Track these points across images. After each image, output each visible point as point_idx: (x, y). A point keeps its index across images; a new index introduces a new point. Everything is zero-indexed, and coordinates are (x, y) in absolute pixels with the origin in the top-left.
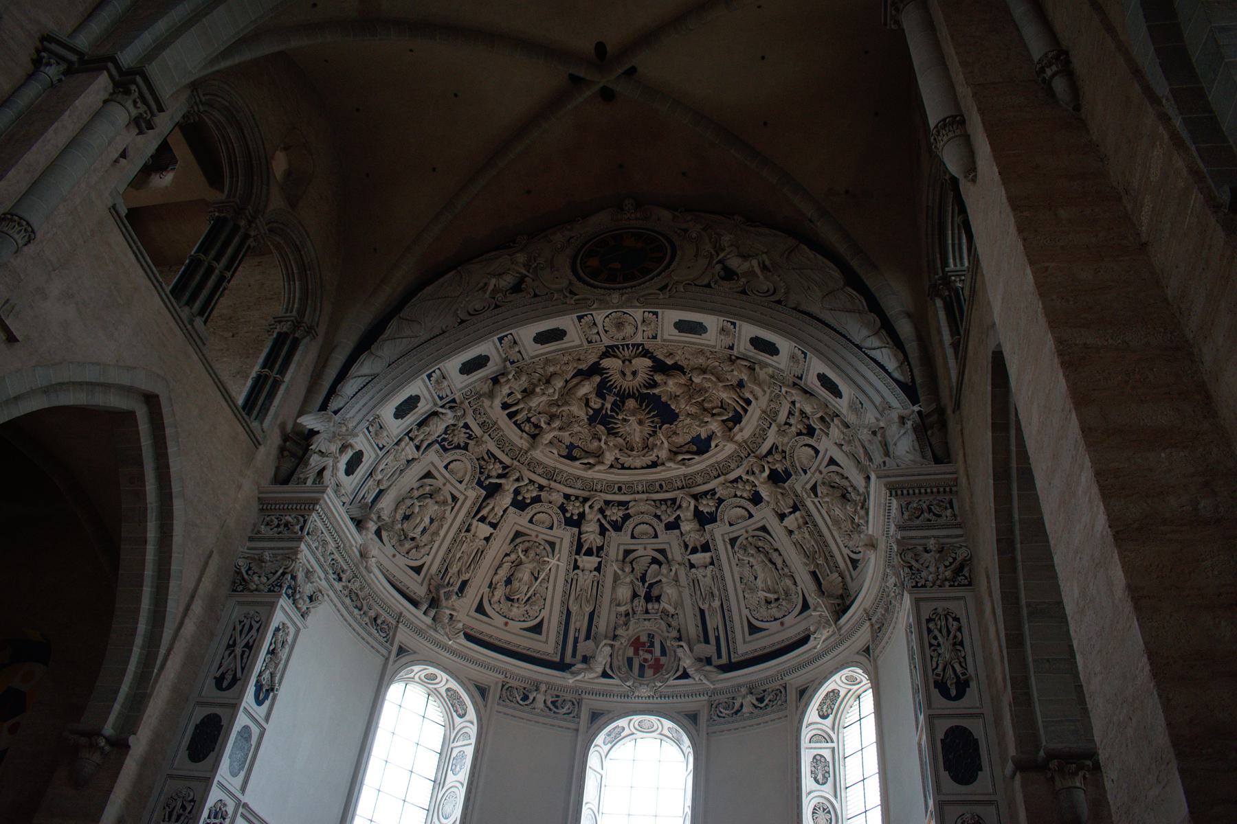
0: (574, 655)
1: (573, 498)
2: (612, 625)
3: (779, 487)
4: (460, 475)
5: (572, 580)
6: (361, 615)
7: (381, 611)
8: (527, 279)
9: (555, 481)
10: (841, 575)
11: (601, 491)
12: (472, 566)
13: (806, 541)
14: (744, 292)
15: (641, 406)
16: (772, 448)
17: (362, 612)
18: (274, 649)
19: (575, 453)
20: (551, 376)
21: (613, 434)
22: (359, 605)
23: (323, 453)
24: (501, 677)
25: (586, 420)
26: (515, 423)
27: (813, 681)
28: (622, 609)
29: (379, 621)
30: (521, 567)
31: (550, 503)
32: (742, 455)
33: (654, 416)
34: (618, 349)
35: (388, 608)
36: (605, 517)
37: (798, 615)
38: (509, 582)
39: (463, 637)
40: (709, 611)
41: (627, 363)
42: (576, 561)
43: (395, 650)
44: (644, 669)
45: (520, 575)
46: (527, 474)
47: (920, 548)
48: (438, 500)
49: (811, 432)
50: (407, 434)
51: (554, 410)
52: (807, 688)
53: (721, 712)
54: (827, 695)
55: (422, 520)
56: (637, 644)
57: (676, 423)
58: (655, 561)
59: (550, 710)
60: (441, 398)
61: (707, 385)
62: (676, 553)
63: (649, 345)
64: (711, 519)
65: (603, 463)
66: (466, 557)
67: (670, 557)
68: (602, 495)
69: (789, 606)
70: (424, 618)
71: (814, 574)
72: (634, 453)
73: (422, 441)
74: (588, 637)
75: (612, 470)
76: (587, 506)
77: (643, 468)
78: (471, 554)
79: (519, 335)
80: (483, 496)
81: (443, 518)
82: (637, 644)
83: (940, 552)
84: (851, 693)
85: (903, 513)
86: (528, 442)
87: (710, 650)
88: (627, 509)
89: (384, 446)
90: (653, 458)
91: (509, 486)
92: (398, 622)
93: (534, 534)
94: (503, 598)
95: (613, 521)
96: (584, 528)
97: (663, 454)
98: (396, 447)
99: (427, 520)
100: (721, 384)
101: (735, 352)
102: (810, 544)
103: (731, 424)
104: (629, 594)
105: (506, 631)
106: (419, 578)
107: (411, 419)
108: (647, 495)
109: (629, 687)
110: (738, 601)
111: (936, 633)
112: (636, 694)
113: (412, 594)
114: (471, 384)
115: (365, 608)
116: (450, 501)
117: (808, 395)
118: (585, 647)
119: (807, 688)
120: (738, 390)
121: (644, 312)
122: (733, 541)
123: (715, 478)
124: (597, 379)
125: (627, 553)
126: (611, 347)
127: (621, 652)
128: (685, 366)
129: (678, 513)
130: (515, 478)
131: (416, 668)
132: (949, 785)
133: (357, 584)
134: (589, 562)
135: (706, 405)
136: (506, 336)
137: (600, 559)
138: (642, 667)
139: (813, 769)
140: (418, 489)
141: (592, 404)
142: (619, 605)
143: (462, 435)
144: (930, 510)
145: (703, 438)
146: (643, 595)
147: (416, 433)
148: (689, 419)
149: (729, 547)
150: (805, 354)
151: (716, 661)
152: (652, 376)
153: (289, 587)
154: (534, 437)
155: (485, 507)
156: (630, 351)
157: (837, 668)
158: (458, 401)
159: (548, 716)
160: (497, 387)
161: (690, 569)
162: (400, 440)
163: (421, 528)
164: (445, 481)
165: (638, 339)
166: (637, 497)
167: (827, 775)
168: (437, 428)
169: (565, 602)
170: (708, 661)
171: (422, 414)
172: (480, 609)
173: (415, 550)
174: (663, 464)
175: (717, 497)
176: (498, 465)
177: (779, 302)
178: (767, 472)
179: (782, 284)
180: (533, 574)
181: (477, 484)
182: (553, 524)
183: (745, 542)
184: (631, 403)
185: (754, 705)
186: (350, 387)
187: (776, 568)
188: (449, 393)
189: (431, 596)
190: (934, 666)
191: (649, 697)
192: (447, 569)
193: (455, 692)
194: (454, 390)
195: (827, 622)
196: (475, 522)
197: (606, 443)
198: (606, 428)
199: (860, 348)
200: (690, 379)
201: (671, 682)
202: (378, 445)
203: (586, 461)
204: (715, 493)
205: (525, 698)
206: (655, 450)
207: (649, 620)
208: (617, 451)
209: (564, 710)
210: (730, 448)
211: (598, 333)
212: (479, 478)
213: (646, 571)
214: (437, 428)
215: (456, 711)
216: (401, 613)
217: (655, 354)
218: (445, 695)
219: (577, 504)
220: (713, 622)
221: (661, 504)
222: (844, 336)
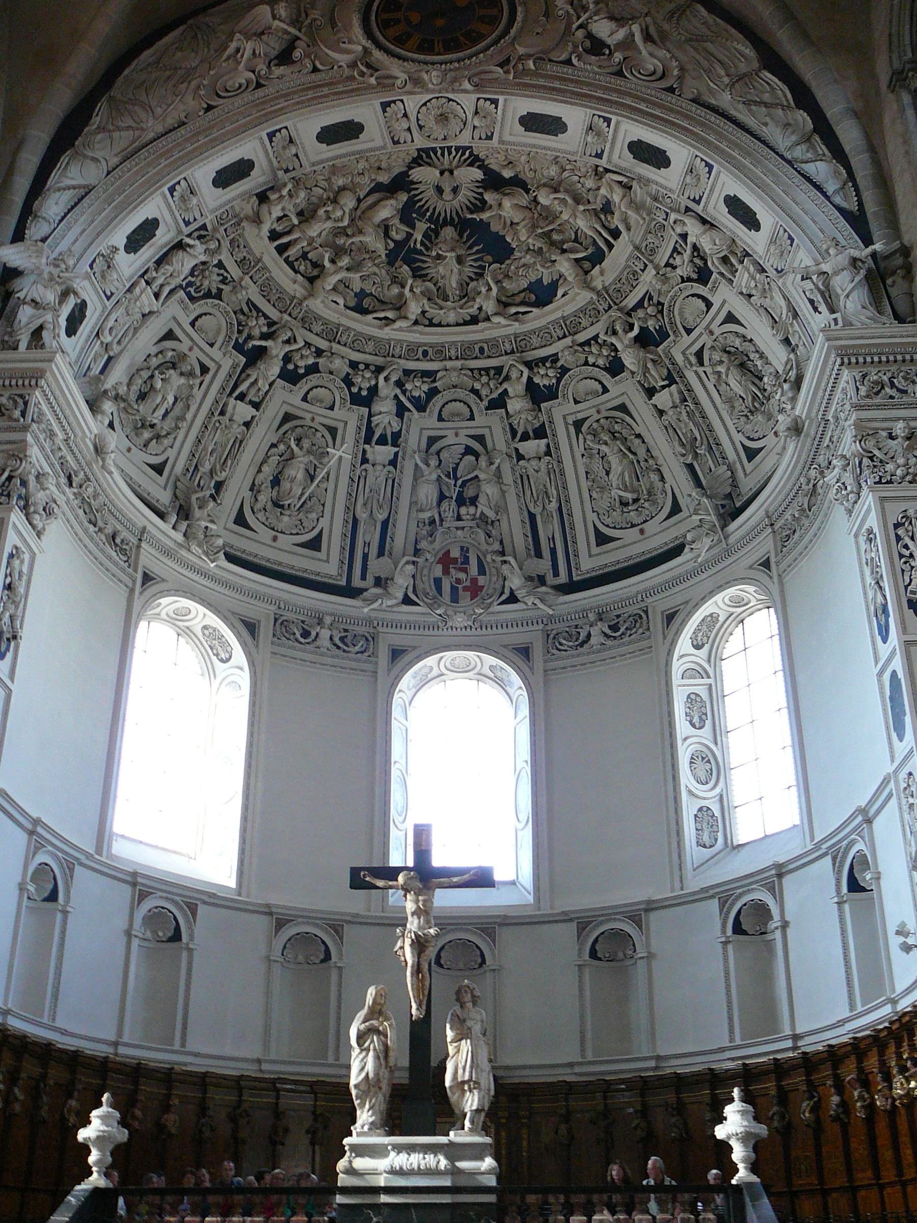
0: (364, 577)
1: (362, 367)
2: (412, 538)
3: (649, 352)
4: (211, 335)
5: (359, 477)
6: (96, 532)
7: (119, 527)
8: (298, 43)
9: (339, 343)
10: (730, 468)
11: (400, 357)
12: (229, 462)
13: (683, 426)
14: (620, 74)
15: (461, 237)
16: (642, 299)
17: (97, 529)
18: (10, 585)
19: (366, 303)
20: (338, 192)
21: (421, 276)
22: (93, 519)
23: (37, 303)
24: (273, 608)
25: (384, 256)
26: (286, 260)
27: (687, 602)
28: (426, 515)
29: (118, 541)
30: (293, 461)
31: (331, 373)
32: (601, 308)
33: (477, 252)
34: (436, 154)
35: (128, 524)
36: (404, 392)
37: (665, 520)
38: (276, 482)
39: (223, 557)
40: (541, 514)
41: (447, 173)
42: (364, 451)
43: (139, 577)
44: (458, 593)
45: (293, 473)
46: (302, 336)
47: (884, 434)
48: (184, 370)
49: (703, 276)
50: (142, 276)
51: (341, 241)
52: (677, 611)
53: (561, 644)
54: (703, 620)
55: (164, 399)
56: (446, 561)
57: (508, 262)
58: (469, 451)
59: (338, 648)
60: (187, 223)
61: (557, 207)
62: (499, 440)
63: (481, 148)
64: (552, 393)
65: (406, 318)
66: (220, 449)
67: (490, 445)
68: (402, 361)
69: (651, 508)
70: (172, 533)
71: (690, 467)
72: (449, 303)
73: (162, 286)
74: (381, 553)
75: (415, 328)
76: (381, 378)
77: (458, 325)
78: (226, 446)
79: (297, 130)
80: (242, 365)
81: (190, 396)
82: (446, 561)
83: (908, 438)
84: (733, 617)
85: (858, 389)
86: (304, 287)
87: (543, 566)
88: (434, 381)
89: (112, 294)
90: (473, 311)
91: (277, 349)
92: (140, 540)
93: (308, 416)
94: (269, 505)
95: (413, 397)
96: (377, 407)
97: (490, 306)
98: (128, 296)
99: (171, 399)
100: (581, 208)
101: (603, 162)
102: (688, 427)
103: (587, 265)
104: (435, 496)
105: (275, 548)
106: (161, 480)
107: (148, 253)
108: (463, 362)
109: (440, 615)
110: (582, 502)
111: (907, 540)
112: (450, 624)
113: (154, 502)
114: (229, 201)
115: (100, 523)
116: (198, 372)
117: (708, 226)
118: (377, 566)
119: (676, 612)
120: (602, 217)
121: (478, 99)
122: (578, 425)
123: (559, 339)
124: (403, 197)
125: (432, 441)
126: (426, 151)
127: (425, 572)
128: (528, 181)
129: (505, 385)
130: (286, 338)
131: (164, 601)
133: (90, 490)
134: (382, 453)
135: (555, 237)
136: (279, 130)
137: (396, 449)
138: (454, 590)
139: (688, 710)
140: (156, 355)
141: (393, 234)
142: (421, 510)
143: (215, 277)
144: (892, 385)
145: (545, 283)
146: (454, 498)
147: (154, 274)
148: (528, 257)
149: (572, 430)
150: (710, 167)
152: (481, 194)
153: (20, 497)
154: (311, 280)
155: (244, 380)
156: (451, 156)
157: (721, 586)
158: (209, 227)
159: (337, 657)
160: (265, 207)
161: (518, 462)
162: (133, 286)
163: (161, 412)
164: (190, 343)
165: (464, 139)
166: (449, 364)
167: (704, 717)
168: (183, 264)
169: (350, 509)
170: (542, 580)
171: (162, 247)
172: (240, 520)
173: (155, 441)
174: (488, 319)
175: (559, 364)
176: (262, 321)
178: (636, 331)
179: (675, 64)
180: (307, 470)
181: (233, 348)
182: (334, 402)
183: (595, 425)
184: (448, 232)
185: (606, 635)
187: (638, 462)
188: (198, 216)
189: (177, 504)
190: (907, 581)
191: (466, 628)
192: (196, 465)
193: (215, 630)
194: (205, 211)
195: (713, 529)
196: (232, 401)
197: (411, 290)
198: (412, 269)
200: (535, 200)
201: (496, 608)
202: (104, 292)
203: (382, 315)
204: (558, 360)
205: (306, 634)
206: (478, 300)
207: (463, 528)
208: (425, 301)
209: (357, 648)
210: (584, 297)
211: (409, 129)
212: (237, 339)
213: (458, 464)
214: (183, 264)
215: (217, 655)
216: (145, 528)
217: (486, 163)
218: (200, 635)
219: (368, 375)
220: (548, 529)
221: (480, 373)
222: (764, 142)
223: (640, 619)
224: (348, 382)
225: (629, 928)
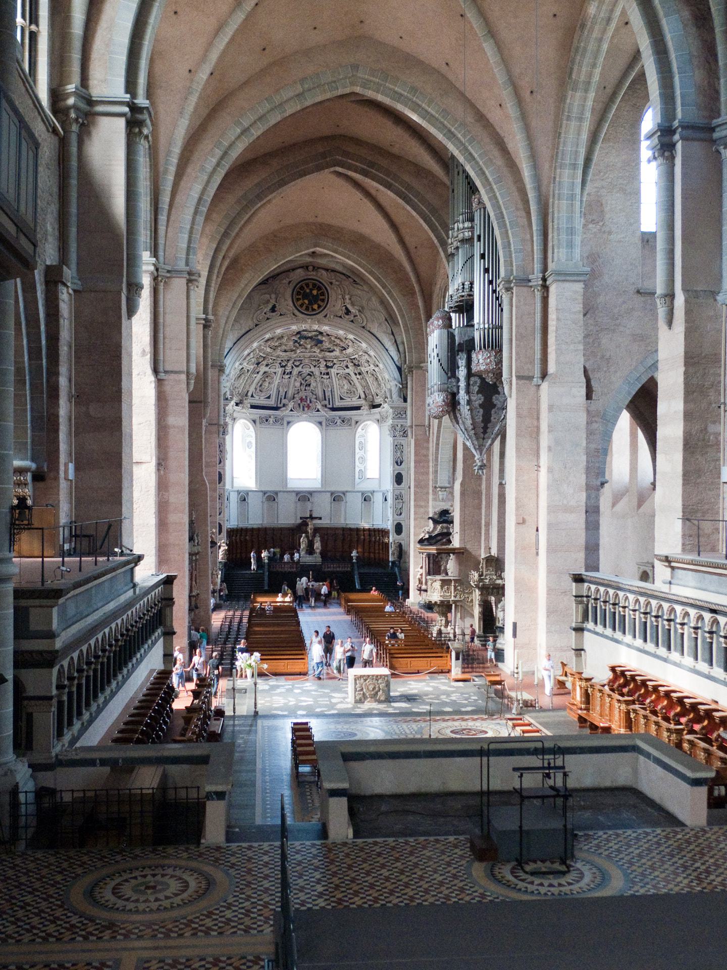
14: (352, 321)
38: (261, 386)
56: (301, 399)
58: (309, 374)
64: (331, 367)
74: (285, 398)
82: (301, 399)
91: (265, 363)
118: (284, 401)
132: (396, 486)
138: (303, 407)
151: (328, 406)
170: (326, 406)
172: (252, 396)
177: (364, 327)
199: (387, 350)
205: (267, 420)
220: (328, 394)
223: (350, 420)
224: (280, 364)
225: (342, 495)
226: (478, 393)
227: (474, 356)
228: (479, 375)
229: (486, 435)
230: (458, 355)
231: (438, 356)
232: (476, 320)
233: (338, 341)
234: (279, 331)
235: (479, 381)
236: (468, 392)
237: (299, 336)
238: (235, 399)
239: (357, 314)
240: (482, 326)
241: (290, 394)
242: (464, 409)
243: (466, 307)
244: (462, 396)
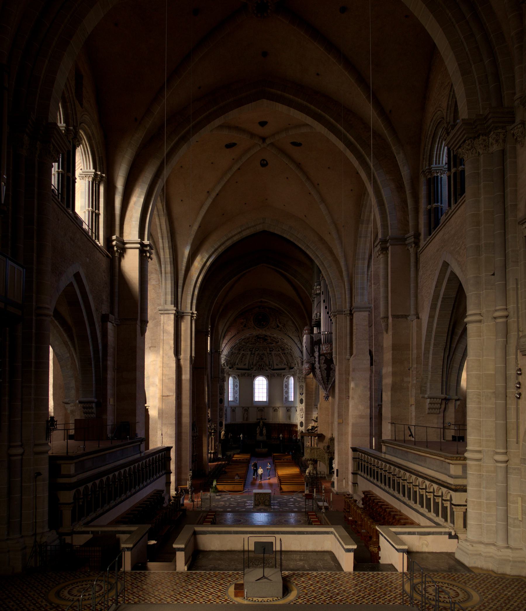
14: (280, 330)
38: (241, 359)
56: (259, 365)
58: (262, 354)
62: (266, 354)
64: (272, 351)
82: (259, 365)
87: (271, 367)
91: (243, 349)
118: (251, 366)
122: (275, 354)
151: (271, 368)
169: (249, 360)
170: (270, 368)
172: (237, 364)
186: (223, 345)
220: (271, 363)
226: (324, 363)
227: (321, 346)
228: (324, 355)
229: (328, 383)
230: (315, 346)
231: (306, 347)
232: (322, 330)
233: (274, 340)
234: (248, 335)
235: (324, 358)
236: (319, 363)
237: (257, 337)
238: (229, 366)
239: (282, 327)
240: (324, 333)
241: (254, 363)
242: (318, 371)
243: (318, 325)
244: (317, 365)
